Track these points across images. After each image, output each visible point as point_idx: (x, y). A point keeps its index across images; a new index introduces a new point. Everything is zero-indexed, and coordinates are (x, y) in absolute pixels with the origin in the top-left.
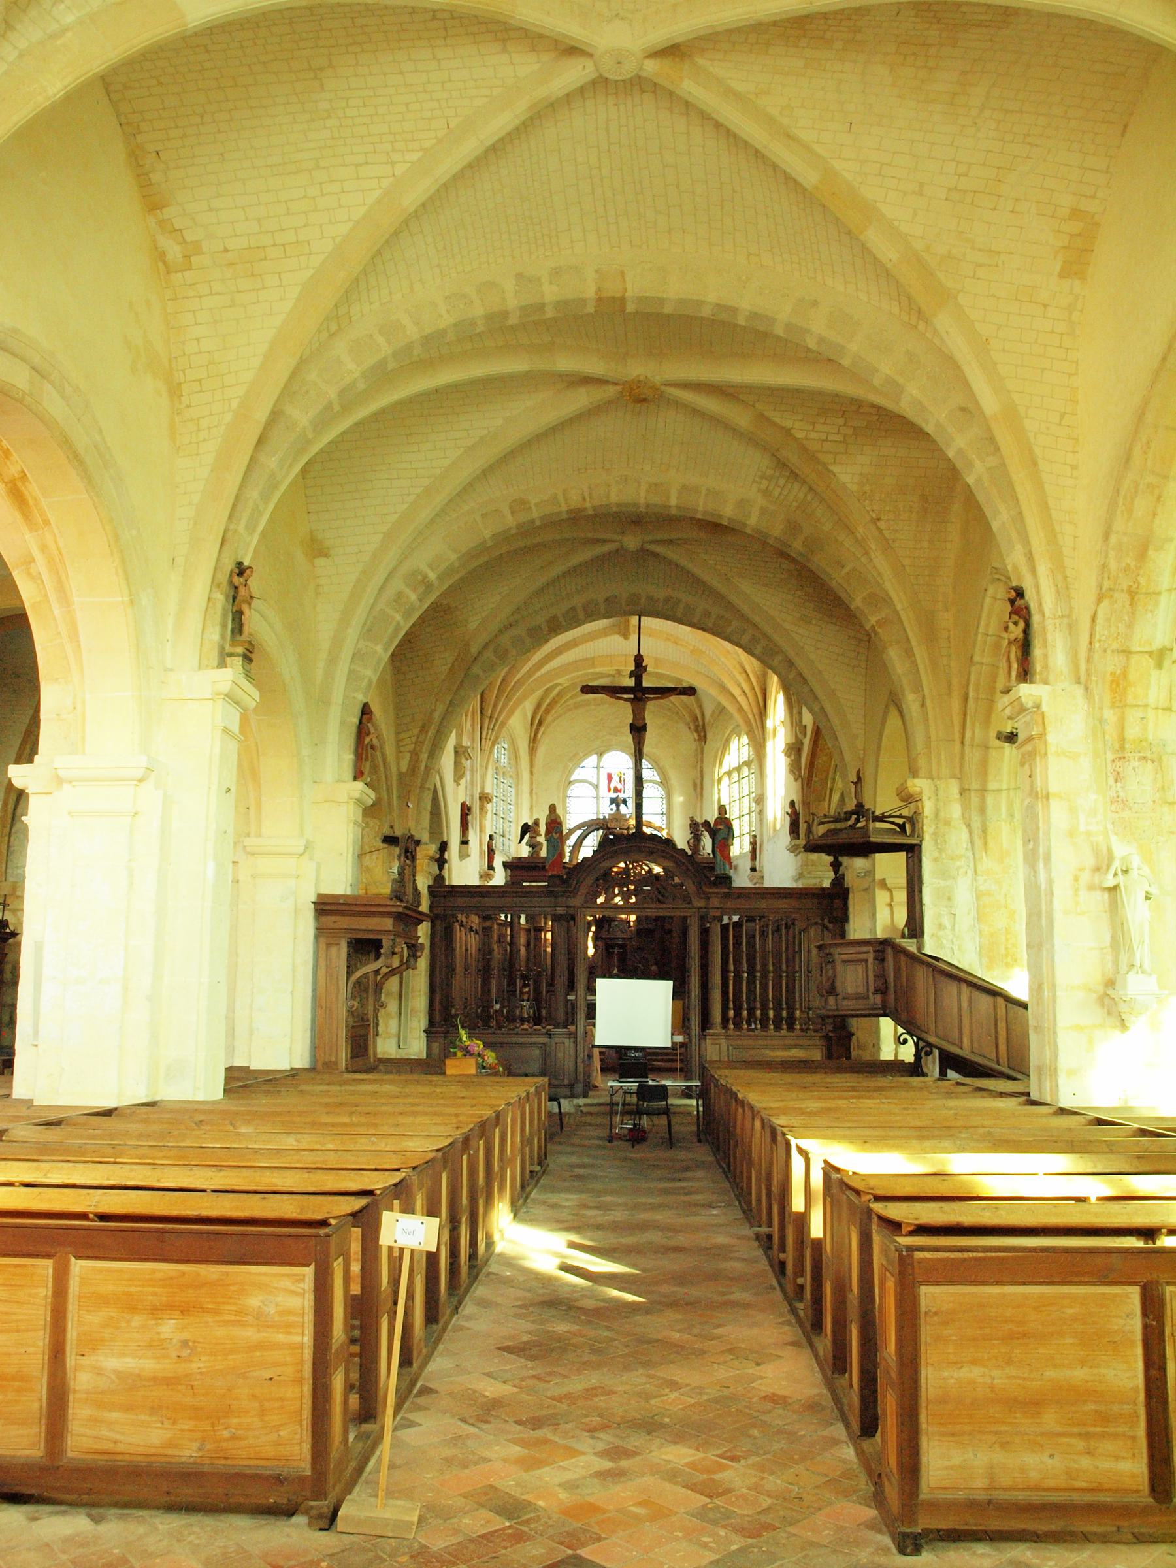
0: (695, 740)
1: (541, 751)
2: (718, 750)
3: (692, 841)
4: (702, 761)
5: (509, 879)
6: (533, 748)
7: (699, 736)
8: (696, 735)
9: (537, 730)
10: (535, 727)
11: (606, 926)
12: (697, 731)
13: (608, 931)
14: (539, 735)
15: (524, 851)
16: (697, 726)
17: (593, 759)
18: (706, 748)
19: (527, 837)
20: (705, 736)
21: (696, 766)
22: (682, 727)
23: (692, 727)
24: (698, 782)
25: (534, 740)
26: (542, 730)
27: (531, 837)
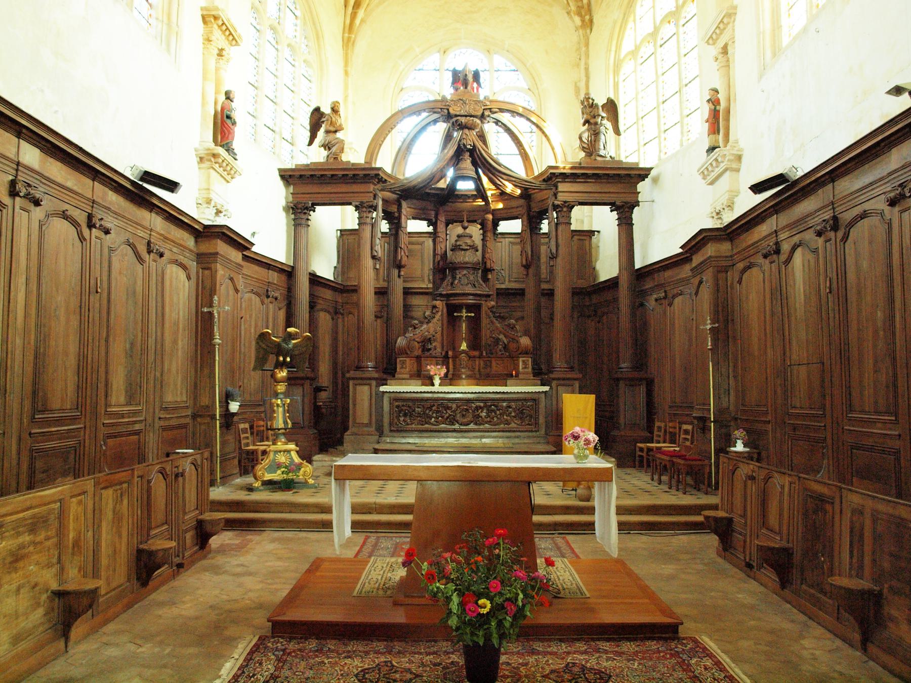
0: (577, 29)
1: (363, 42)
2: (615, 23)
3: (585, 136)
4: (587, 55)
5: (291, 199)
6: (349, 38)
7: (583, 21)
8: (577, 20)
9: (354, 16)
10: (350, 9)
11: (449, 278)
12: (579, 14)
13: (452, 284)
14: (358, 21)
15: (316, 155)
16: (580, 8)
17: (434, 59)
18: (593, 37)
19: (321, 134)
20: (591, 21)
21: (578, 65)
22: (559, 14)
23: (573, 8)
24: (582, 85)
25: (350, 28)
26: (361, 13)
27: (327, 132)
